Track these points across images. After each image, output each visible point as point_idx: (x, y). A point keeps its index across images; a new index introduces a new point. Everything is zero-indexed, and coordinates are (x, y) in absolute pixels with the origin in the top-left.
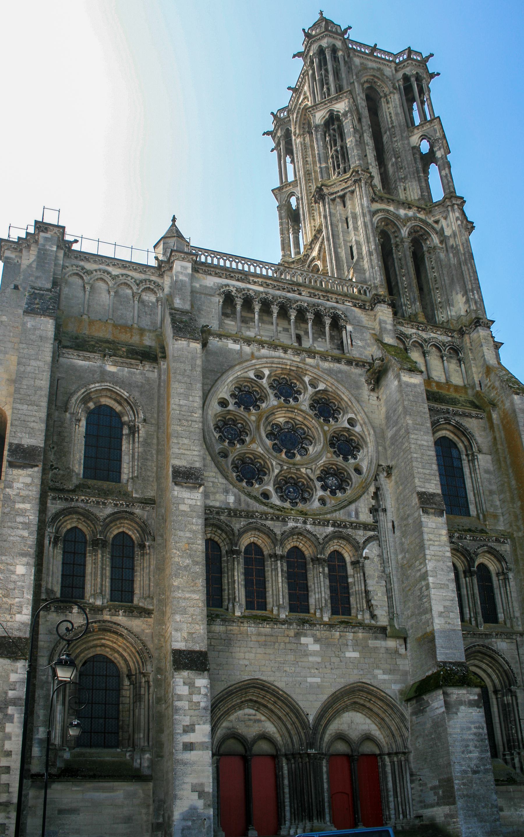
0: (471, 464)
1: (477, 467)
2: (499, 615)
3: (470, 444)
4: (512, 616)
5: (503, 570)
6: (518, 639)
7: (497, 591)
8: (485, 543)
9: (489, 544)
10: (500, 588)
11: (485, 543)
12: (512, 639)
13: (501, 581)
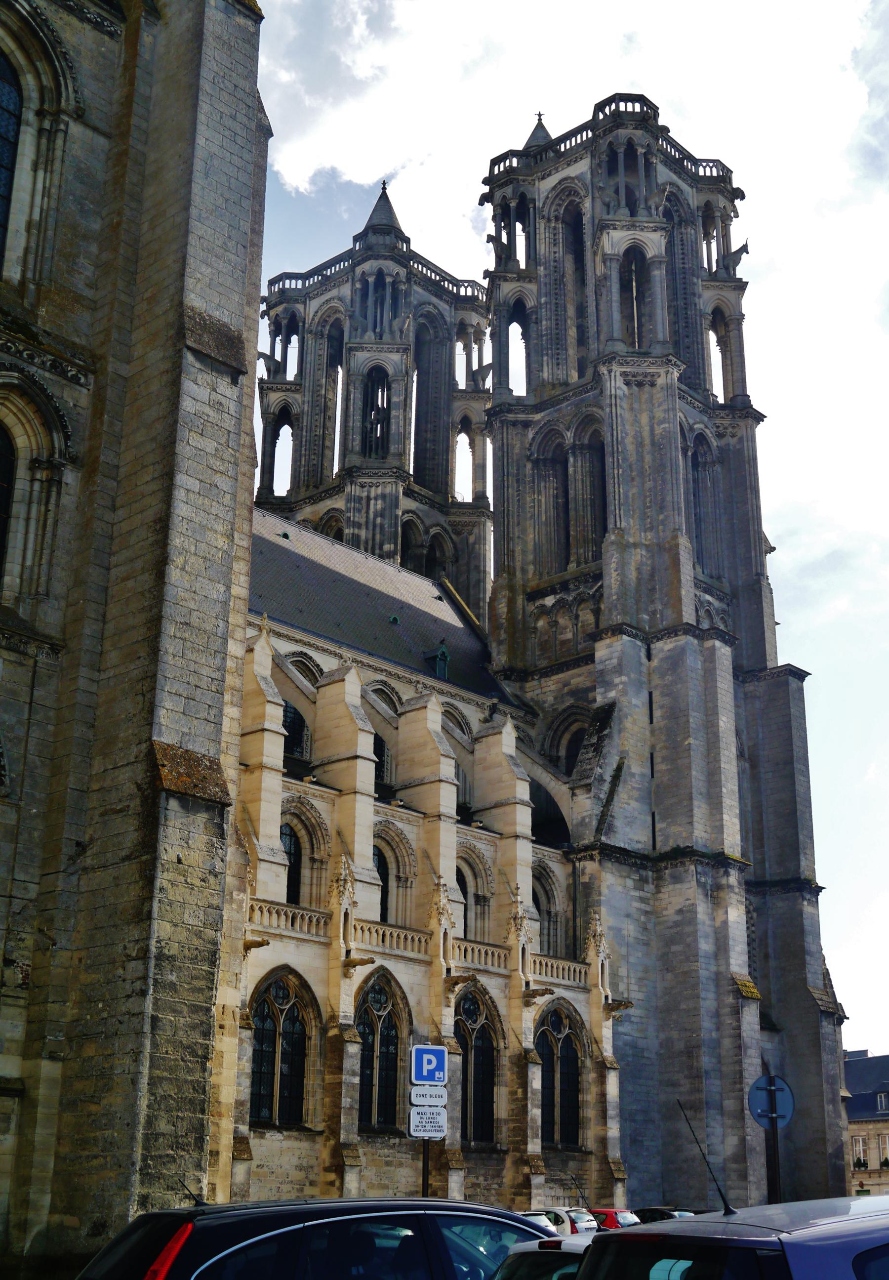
0: (44, 141)
1: (58, 153)
2: (7, 579)
3: (58, 86)
4: (41, 589)
5: (52, 455)
6: (42, 658)
7: (18, 509)
8: (19, 362)
9: (33, 369)
10: (30, 503)
11: (19, 362)
12: (24, 654)
13: (37, 486)
